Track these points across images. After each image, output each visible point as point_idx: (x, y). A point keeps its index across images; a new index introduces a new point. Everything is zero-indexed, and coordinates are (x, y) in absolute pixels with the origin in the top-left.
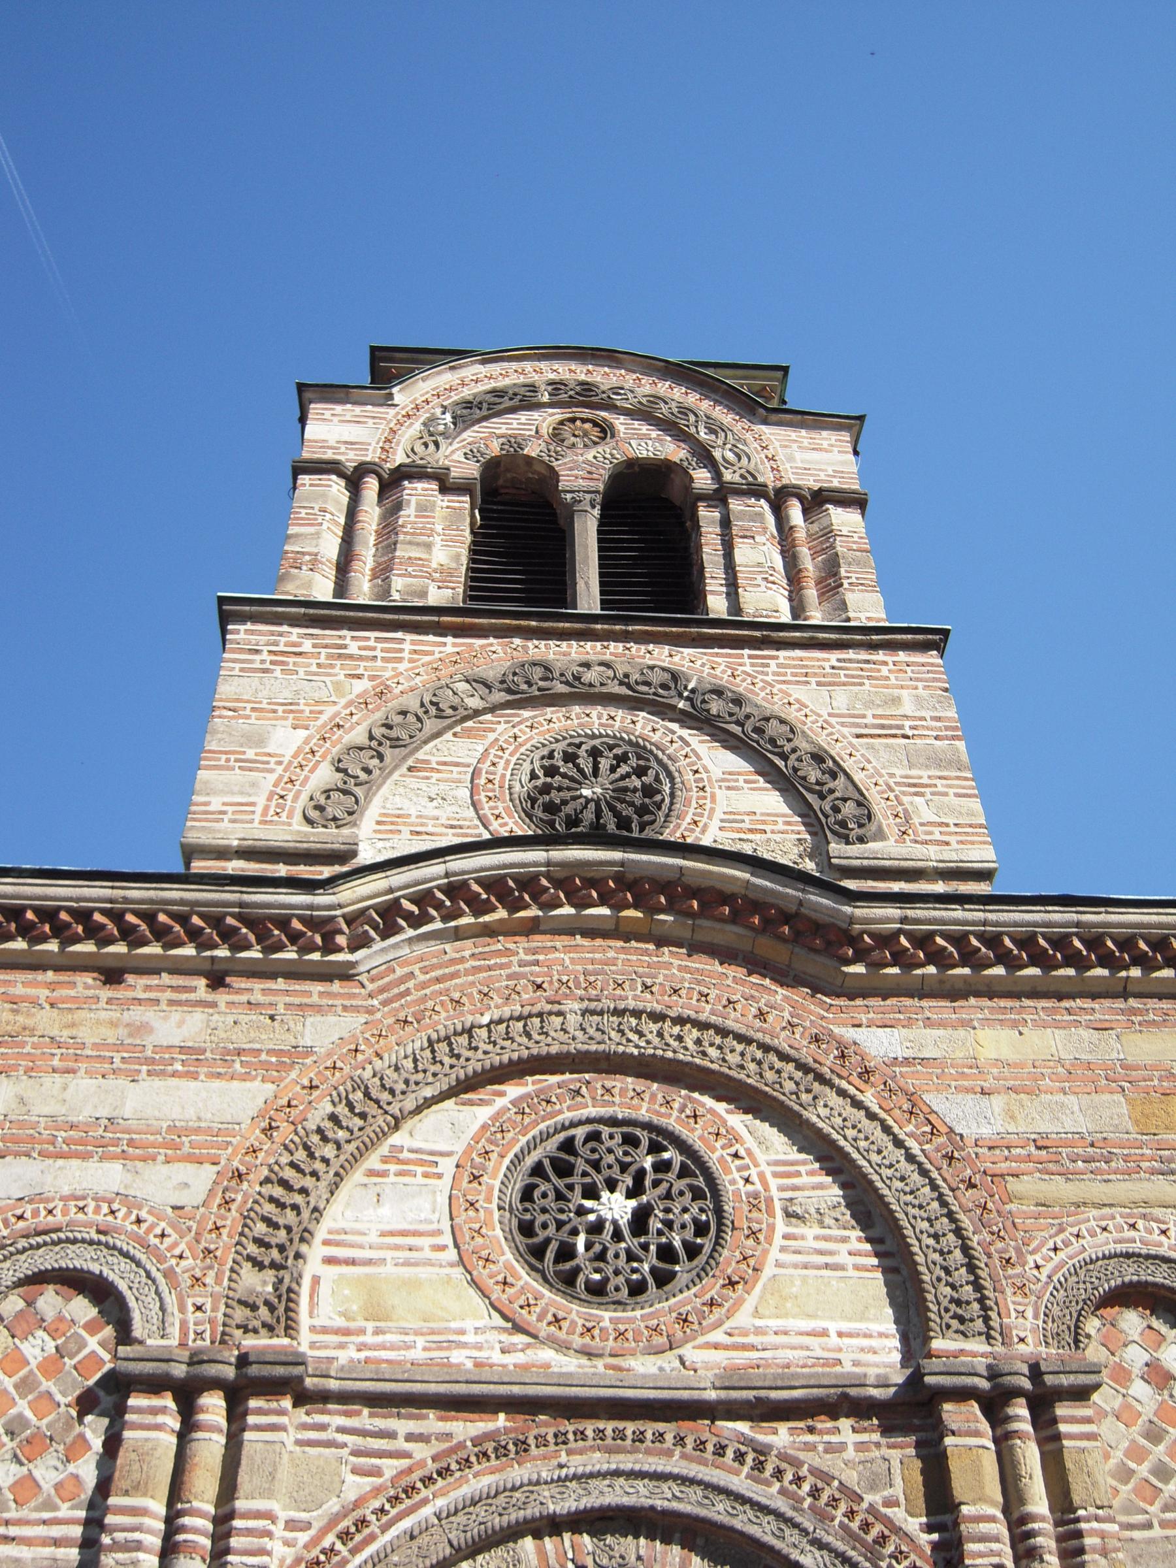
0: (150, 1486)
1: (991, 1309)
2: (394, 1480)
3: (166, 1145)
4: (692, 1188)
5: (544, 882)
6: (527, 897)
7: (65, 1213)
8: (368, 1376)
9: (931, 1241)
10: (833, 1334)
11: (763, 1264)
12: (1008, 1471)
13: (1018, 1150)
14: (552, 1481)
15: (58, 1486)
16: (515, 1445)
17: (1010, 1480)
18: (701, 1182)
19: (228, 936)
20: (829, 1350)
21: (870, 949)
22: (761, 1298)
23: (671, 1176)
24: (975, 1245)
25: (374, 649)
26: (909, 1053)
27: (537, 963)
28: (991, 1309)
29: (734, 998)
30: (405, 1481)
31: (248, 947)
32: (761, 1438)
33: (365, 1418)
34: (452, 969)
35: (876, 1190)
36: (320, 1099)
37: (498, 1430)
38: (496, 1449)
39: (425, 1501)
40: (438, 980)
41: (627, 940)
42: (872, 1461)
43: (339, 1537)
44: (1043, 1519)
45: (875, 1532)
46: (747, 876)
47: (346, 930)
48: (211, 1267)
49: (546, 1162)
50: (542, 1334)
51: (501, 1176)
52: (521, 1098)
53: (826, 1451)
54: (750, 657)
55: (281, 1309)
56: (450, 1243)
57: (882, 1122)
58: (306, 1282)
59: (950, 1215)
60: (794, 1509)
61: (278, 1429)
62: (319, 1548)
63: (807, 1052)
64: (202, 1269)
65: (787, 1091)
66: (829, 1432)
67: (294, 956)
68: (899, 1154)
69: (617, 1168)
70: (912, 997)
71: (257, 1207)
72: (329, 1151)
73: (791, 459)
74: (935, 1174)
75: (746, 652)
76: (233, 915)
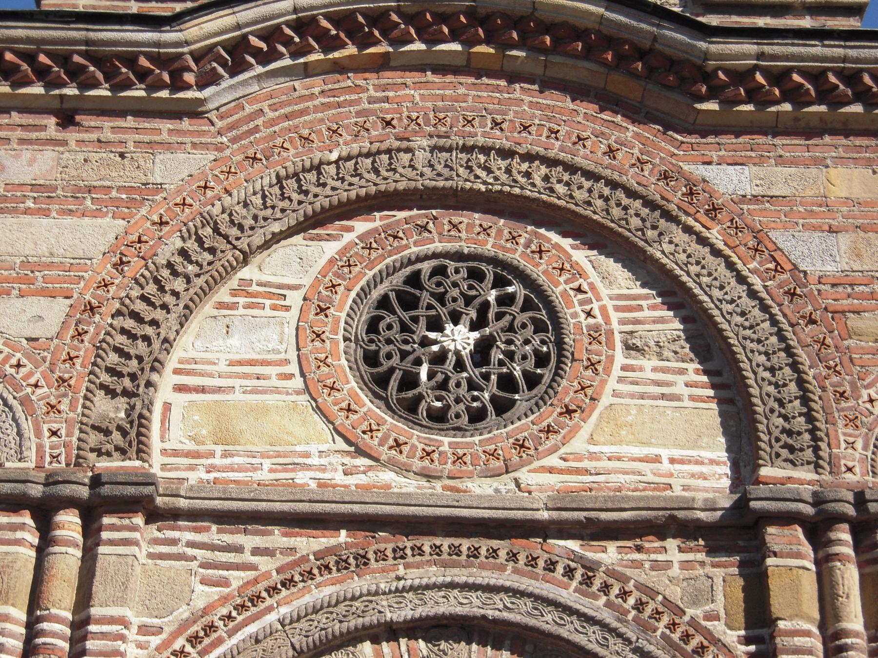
0: (11, 595)
1: (821, 440)
2: (240, 590)
3: (20, 280)
4: (534, 320)
5: (394, 17)
6: (376, 33)
8: (216, 495)
9: (767, 375)
10: (665, 461)
11: (600, 394)
12: (827, 591)
13: (861, 288)
14: (390, 592)
16: (356, 558)
17: (828, 598)
18: (543, 315)
19: (76, 74)
20: (660, 475)
21: (726, 86)
22: (597, 425)
23: (515, 309)
24: (810, 379)
26: (758, 191)
27: (387, 100)
28: (821, 440)
29: (585, 134)
30: (251, 591)
31: (96, 85)
32: (590, 555)
33: (214, 534)
35: (716, 324)
36: (170, 234)
37: (340, 545)
38: (337, 563)
39: (270, 609)
40: (287, 117)
41: (479, 77)
42: (695, 579)
43: (188, 641)
44: (857, 635)
45: (694, 643)
46: (601, 10)
47: (195, 68)
48: (65, 395)
49: (392, 296)
50: (384, 457)
51: (347, 308)
52: (368, 233)
53: (652, 568)
55: (133, 434)
56: (297, 372)
57: (727, 258)
58: (157, 409)
59: (788, 350)
60: (619, 620)
61: (131, 544)
62: (170, 650)
63: (655, 190)
64: (57, 397)
65: (632, 227)
66: (656, 551)
67: (142, 93)
68: (742, 289)
69: (461, 302)
70: (766, 134)
71: (108, 338)
72: (179, 285)
74: (775, 310)
76: (79, 53)
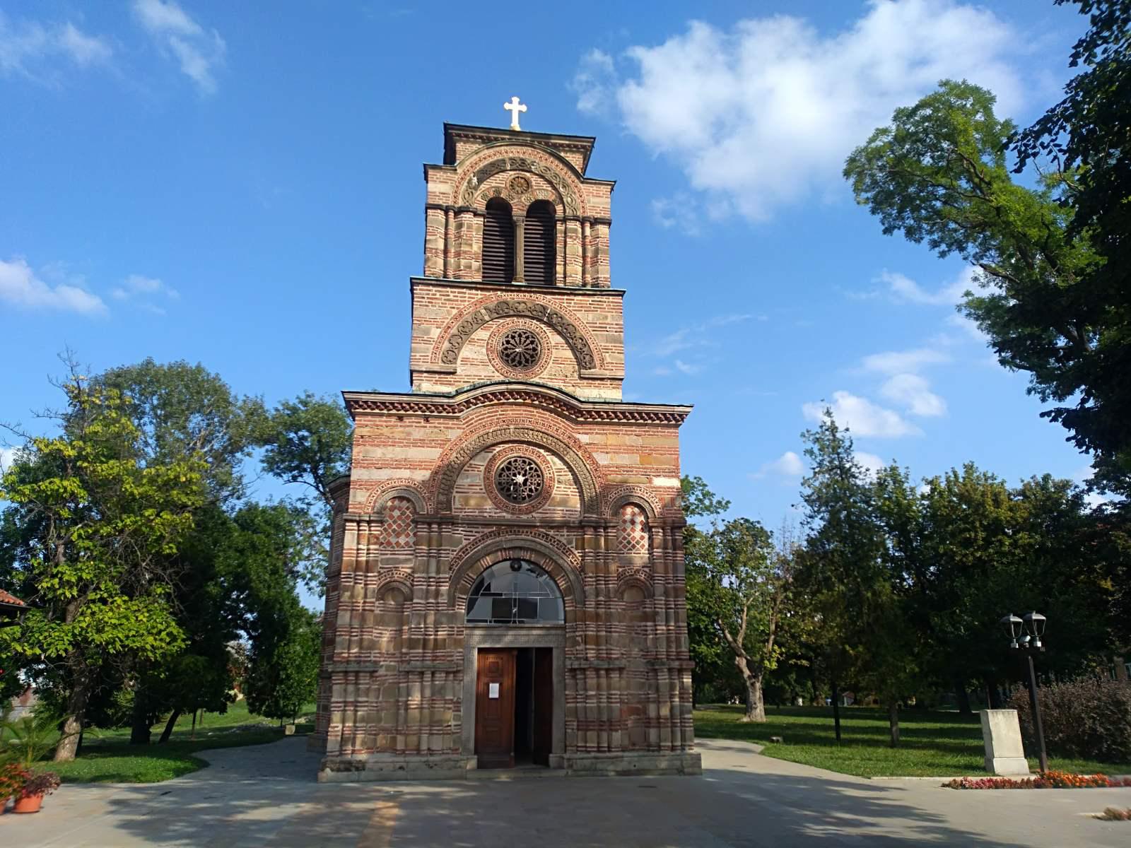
73: (589, 202)
75: (565, 297)
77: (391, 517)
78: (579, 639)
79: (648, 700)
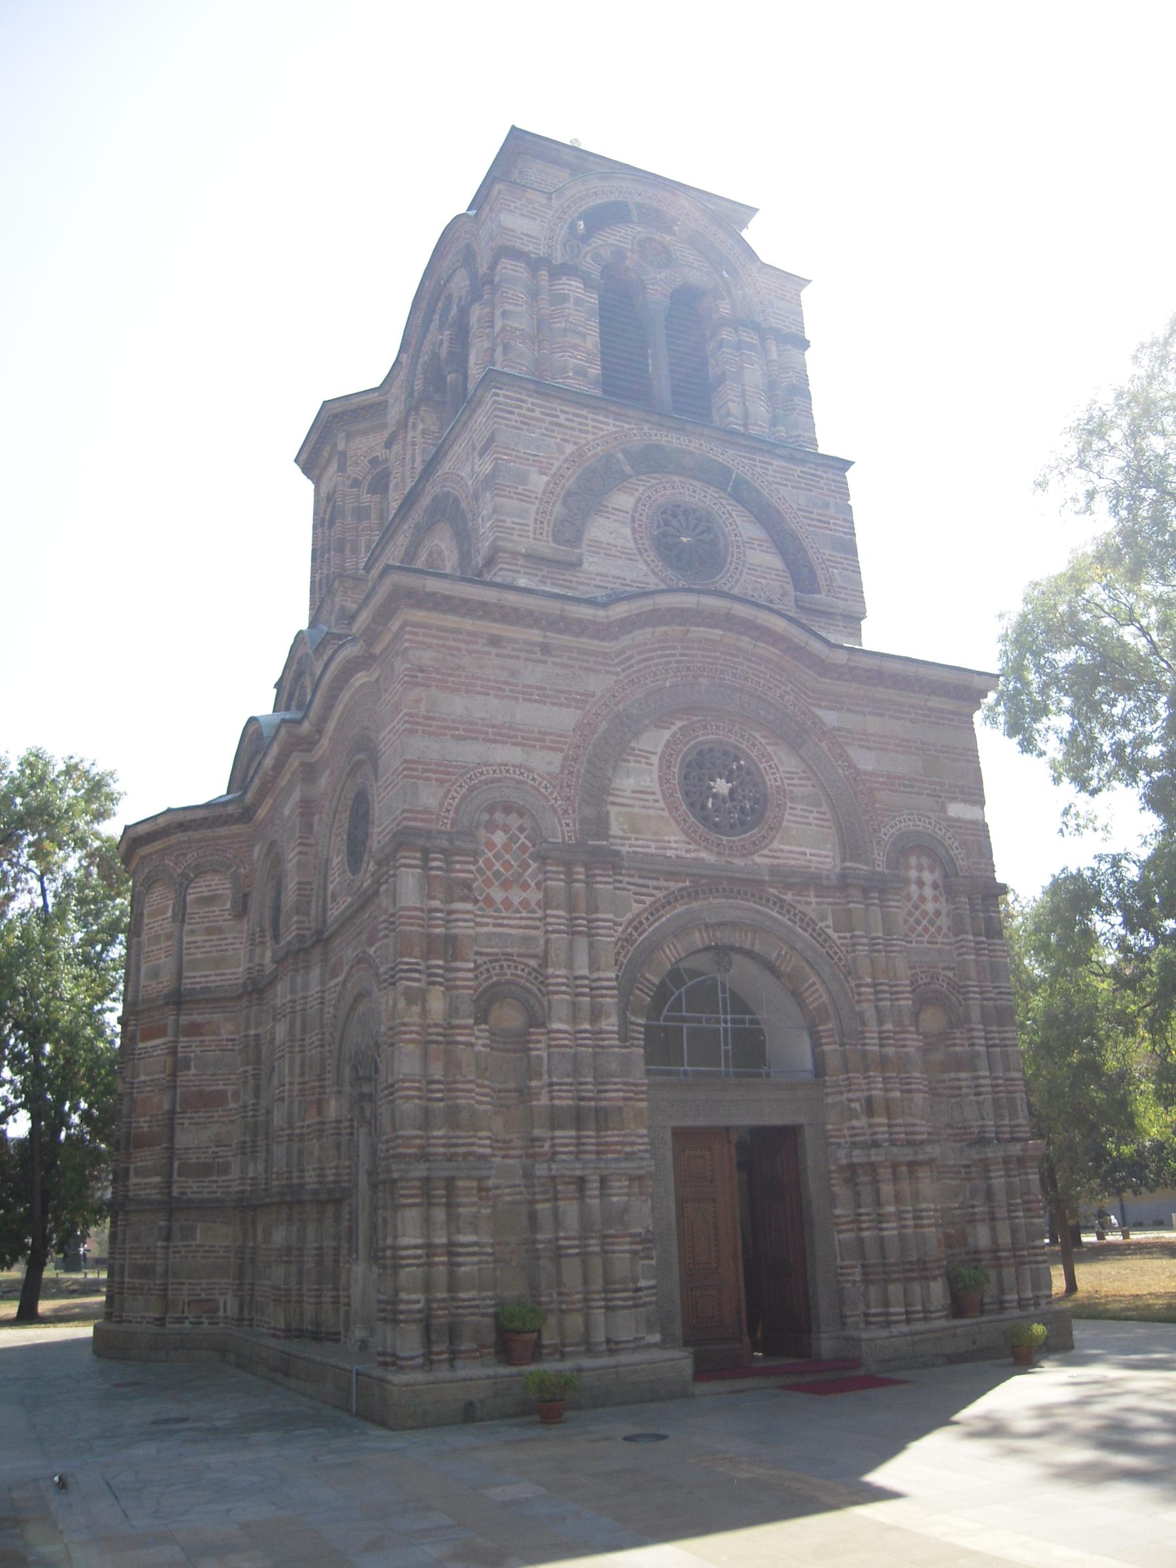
7: (501, 772)
15: (520, 903)
25: (573, 421)
34: (650, 655)
39: (662, 916)
40: (645, 660)
54: (761, 461)
75: (758, 458)
77: (491, 845)
78: (856, 1105)
79: (972, 1220)
